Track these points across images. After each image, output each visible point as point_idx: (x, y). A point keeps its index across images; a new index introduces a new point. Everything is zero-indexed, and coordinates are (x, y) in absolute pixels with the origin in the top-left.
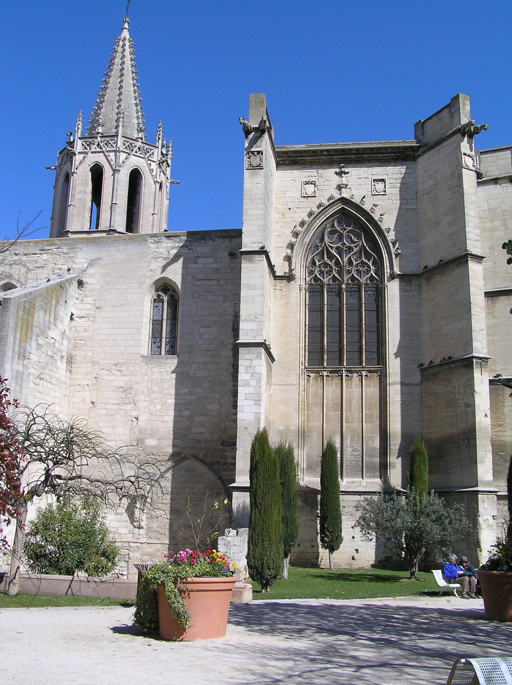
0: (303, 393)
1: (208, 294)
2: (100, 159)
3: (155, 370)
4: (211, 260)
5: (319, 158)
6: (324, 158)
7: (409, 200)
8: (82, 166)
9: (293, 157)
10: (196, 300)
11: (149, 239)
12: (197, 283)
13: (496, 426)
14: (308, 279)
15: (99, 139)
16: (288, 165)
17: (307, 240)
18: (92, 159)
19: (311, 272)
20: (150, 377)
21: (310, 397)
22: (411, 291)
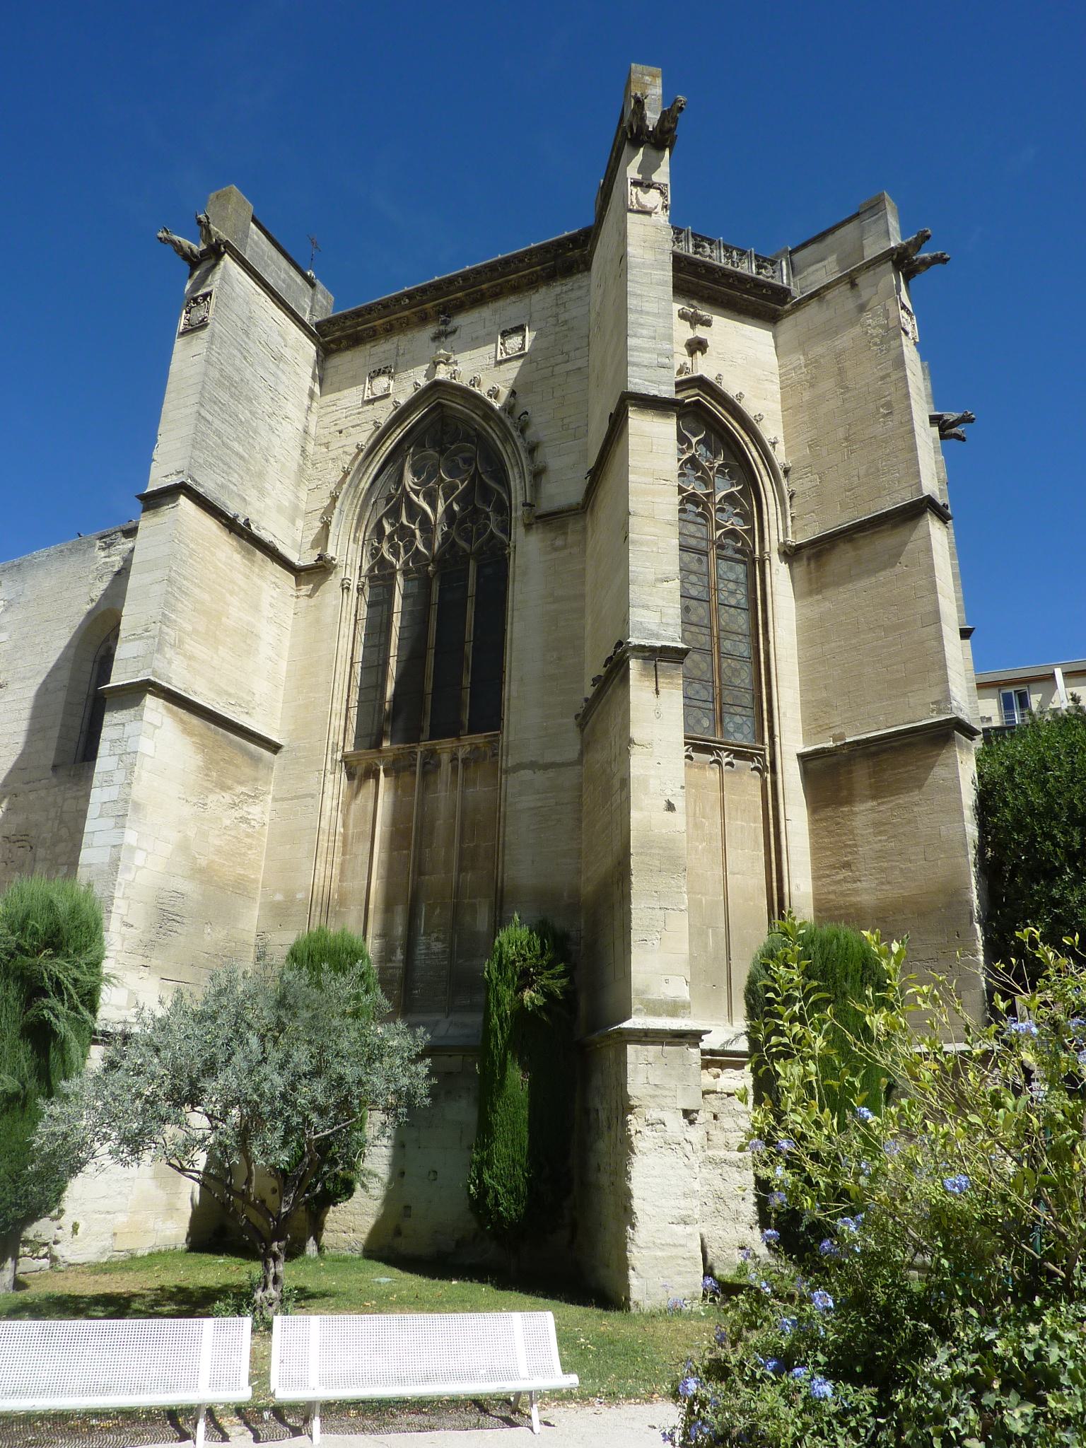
0: (334, 813)
5: (398, 315)
6: (406, 313)
7: (572, 354)
9: (351, 327)
13: (835, 868)
14: (366, 567)
16: (347, 348)
17: (365, 484)
19: (375, 553)
21: (351, 822)
22: (565, 547)
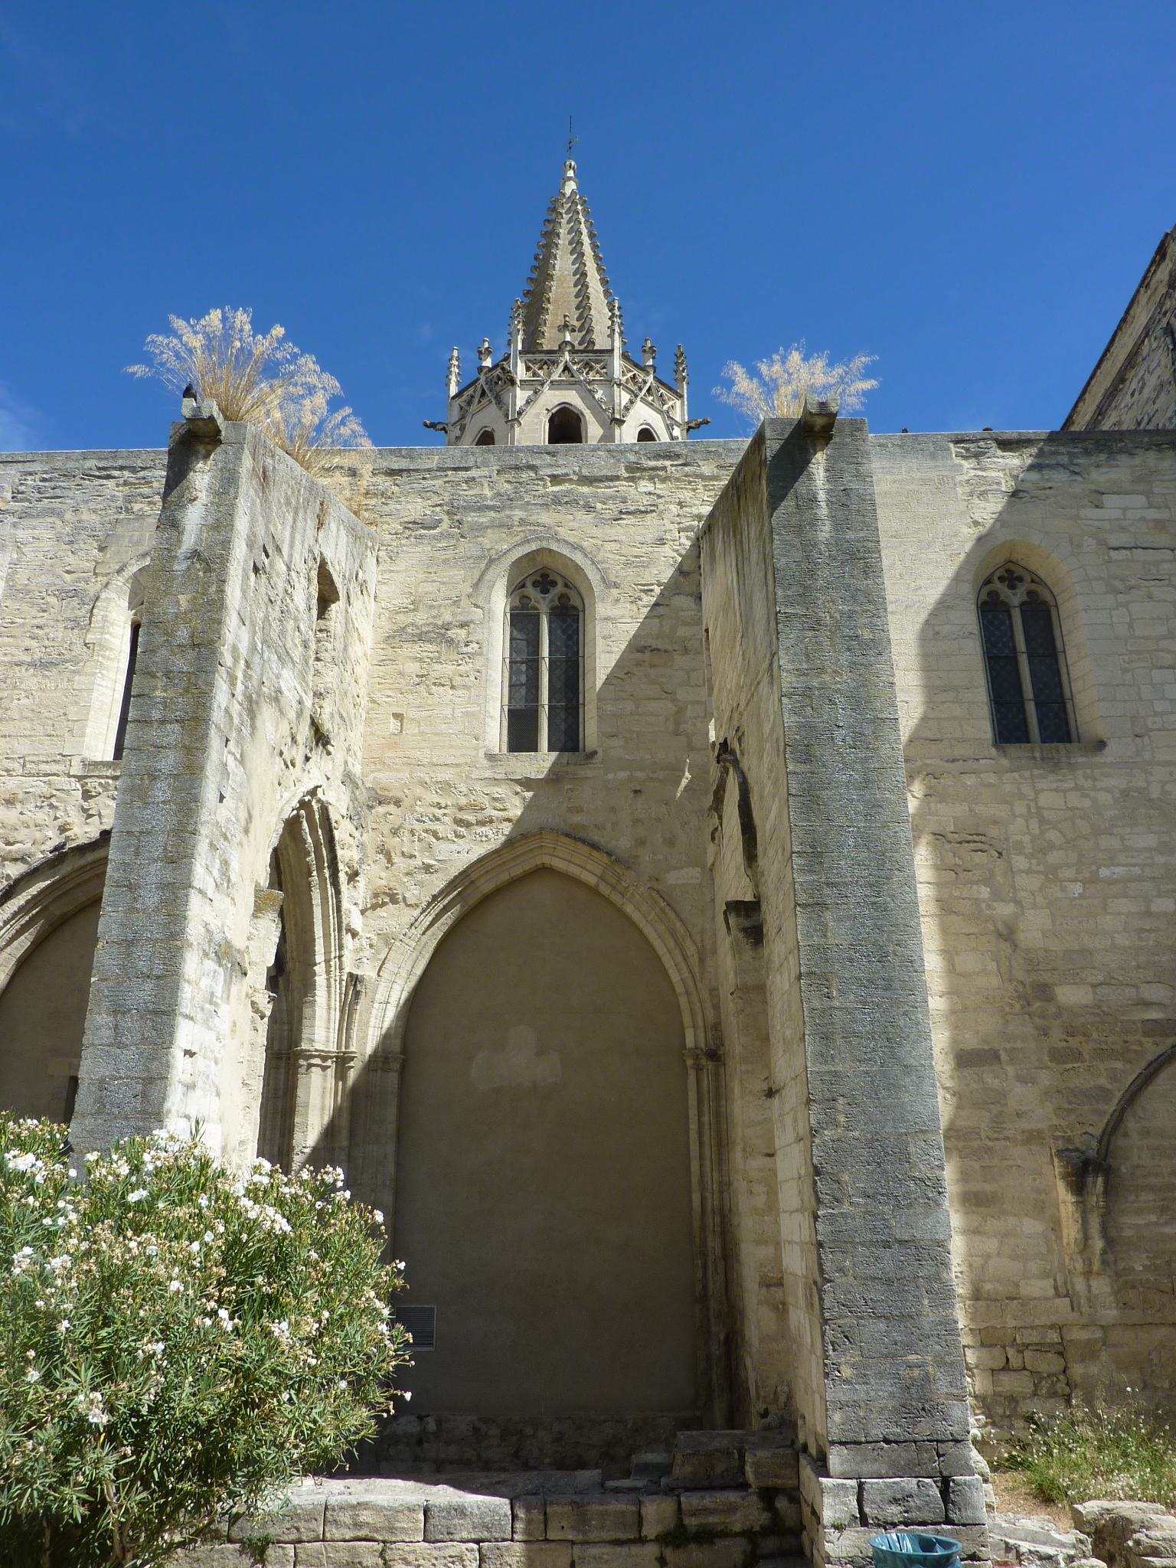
1: (1153, 583)
2: (573, 398)
3: (1042, 784)
4: (1141, 500)
8: (532, 411)
10: (1121, 598)
11: (951, 445)
12: (1113, 554)
15: (567, 356)
18: (551, 399)
20: (1032, 804)
